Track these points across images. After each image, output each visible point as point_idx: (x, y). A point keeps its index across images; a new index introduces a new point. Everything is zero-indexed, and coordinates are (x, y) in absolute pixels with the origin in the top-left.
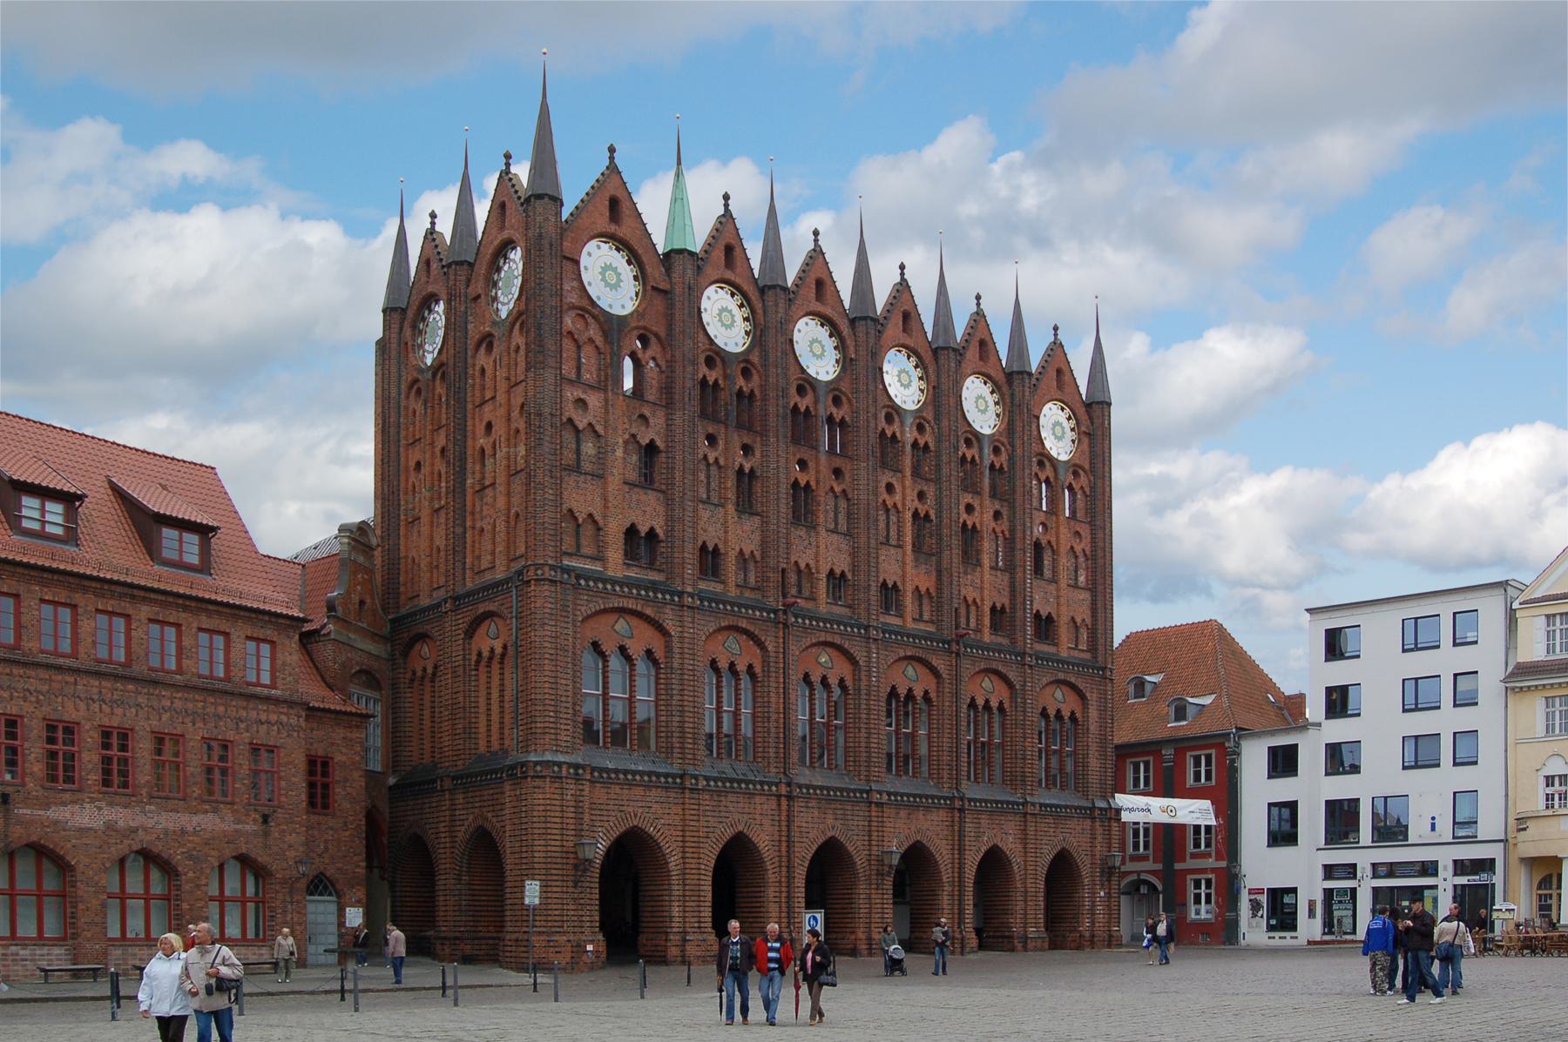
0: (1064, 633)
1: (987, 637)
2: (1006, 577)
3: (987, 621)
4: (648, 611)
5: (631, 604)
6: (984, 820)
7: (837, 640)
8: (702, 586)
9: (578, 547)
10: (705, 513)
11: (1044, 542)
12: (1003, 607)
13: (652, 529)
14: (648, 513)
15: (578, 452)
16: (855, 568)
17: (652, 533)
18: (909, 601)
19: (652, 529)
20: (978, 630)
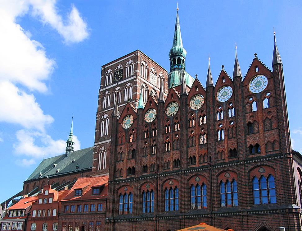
0: (262, 148)
1: (227, 161)
2: (235, 140)
3: (226, 155)
4: (128, 184)
5: (125, 184)
6: (223, 220)
7: (172, 177)
8: (143, 175)
9: (120, 175)
10: (144, 159)
11: (252, 121)
12: (235, 149)
13: (133, 167)
14: (132, 163)
15: (121, 157)
16: (180, 157)
17: (133, 167)
18: (197, 160)
19: (133, 167)
20: (225, 159)
